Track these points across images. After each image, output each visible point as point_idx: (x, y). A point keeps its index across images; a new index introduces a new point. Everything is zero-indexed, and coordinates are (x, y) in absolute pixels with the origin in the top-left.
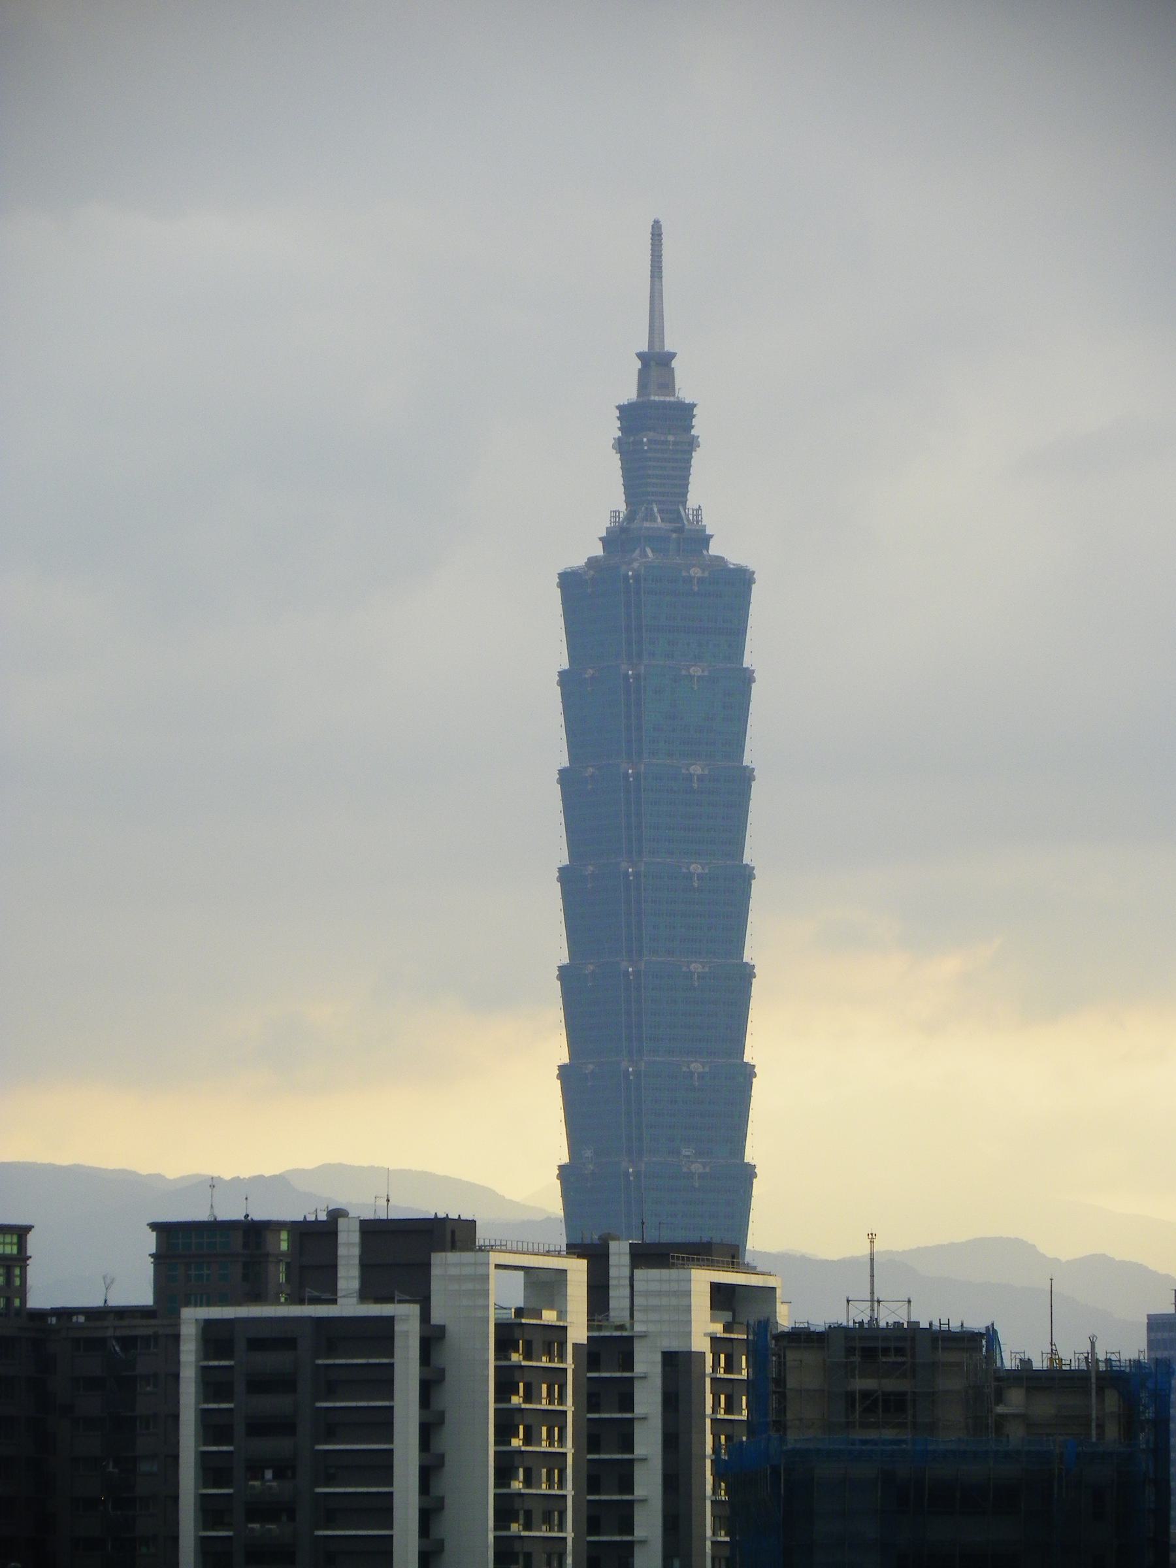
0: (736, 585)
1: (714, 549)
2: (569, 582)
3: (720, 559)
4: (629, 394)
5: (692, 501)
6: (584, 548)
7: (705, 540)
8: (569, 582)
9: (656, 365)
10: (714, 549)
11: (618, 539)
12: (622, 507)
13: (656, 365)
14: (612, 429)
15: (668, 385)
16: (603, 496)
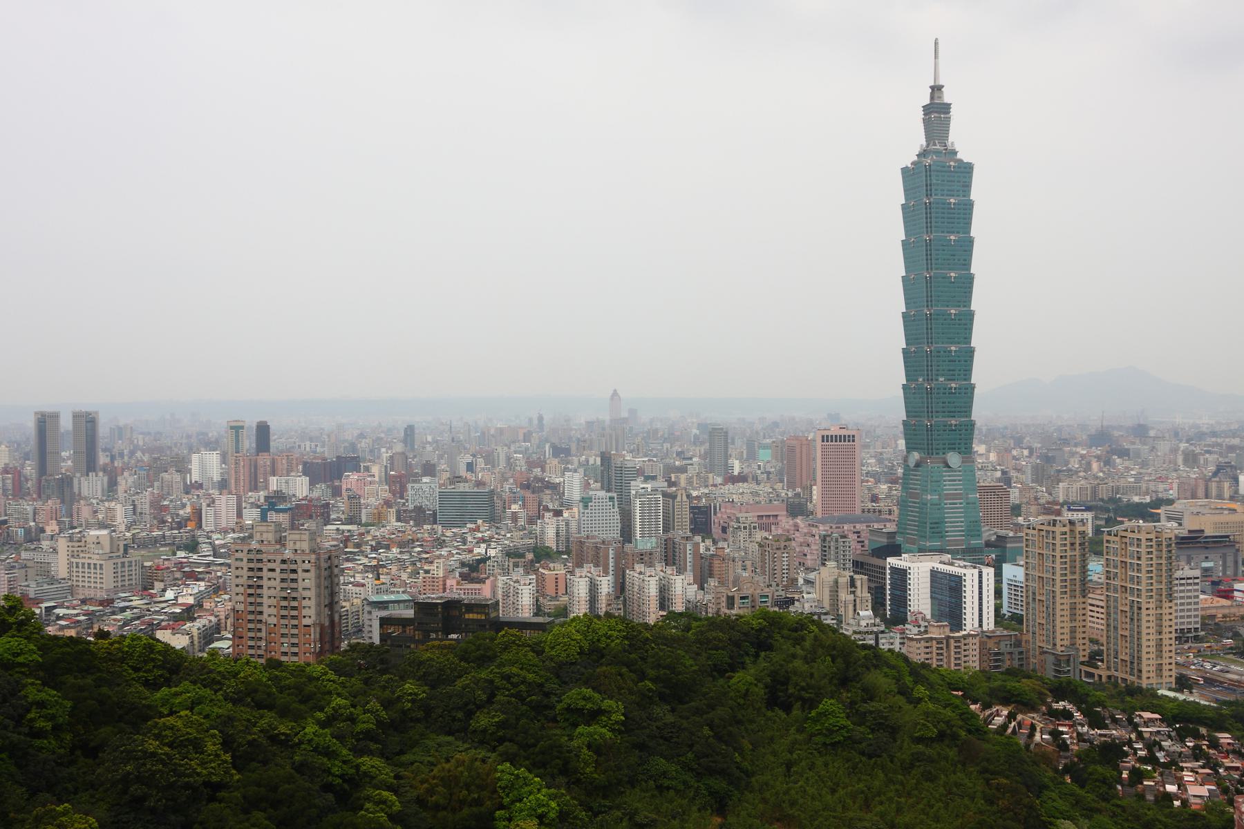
0: (967, 169)
1: (959, 156)
2: (905, 171)
3: (961, 161)
4: (928, 102)
5: (951, 139)
6: (909, 158)
7: (955, 153)
8: (905, 171)
9: (936, 89)
10: (959, 156)
11: (923, 154)
12: (924, 143)
13: (936, 89)
14: (921, 114)
15: (940, 97)
16: (918, 140)
